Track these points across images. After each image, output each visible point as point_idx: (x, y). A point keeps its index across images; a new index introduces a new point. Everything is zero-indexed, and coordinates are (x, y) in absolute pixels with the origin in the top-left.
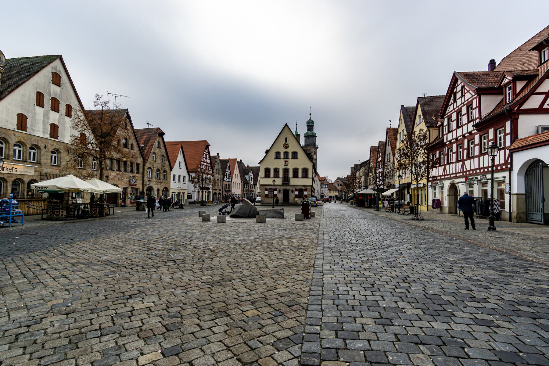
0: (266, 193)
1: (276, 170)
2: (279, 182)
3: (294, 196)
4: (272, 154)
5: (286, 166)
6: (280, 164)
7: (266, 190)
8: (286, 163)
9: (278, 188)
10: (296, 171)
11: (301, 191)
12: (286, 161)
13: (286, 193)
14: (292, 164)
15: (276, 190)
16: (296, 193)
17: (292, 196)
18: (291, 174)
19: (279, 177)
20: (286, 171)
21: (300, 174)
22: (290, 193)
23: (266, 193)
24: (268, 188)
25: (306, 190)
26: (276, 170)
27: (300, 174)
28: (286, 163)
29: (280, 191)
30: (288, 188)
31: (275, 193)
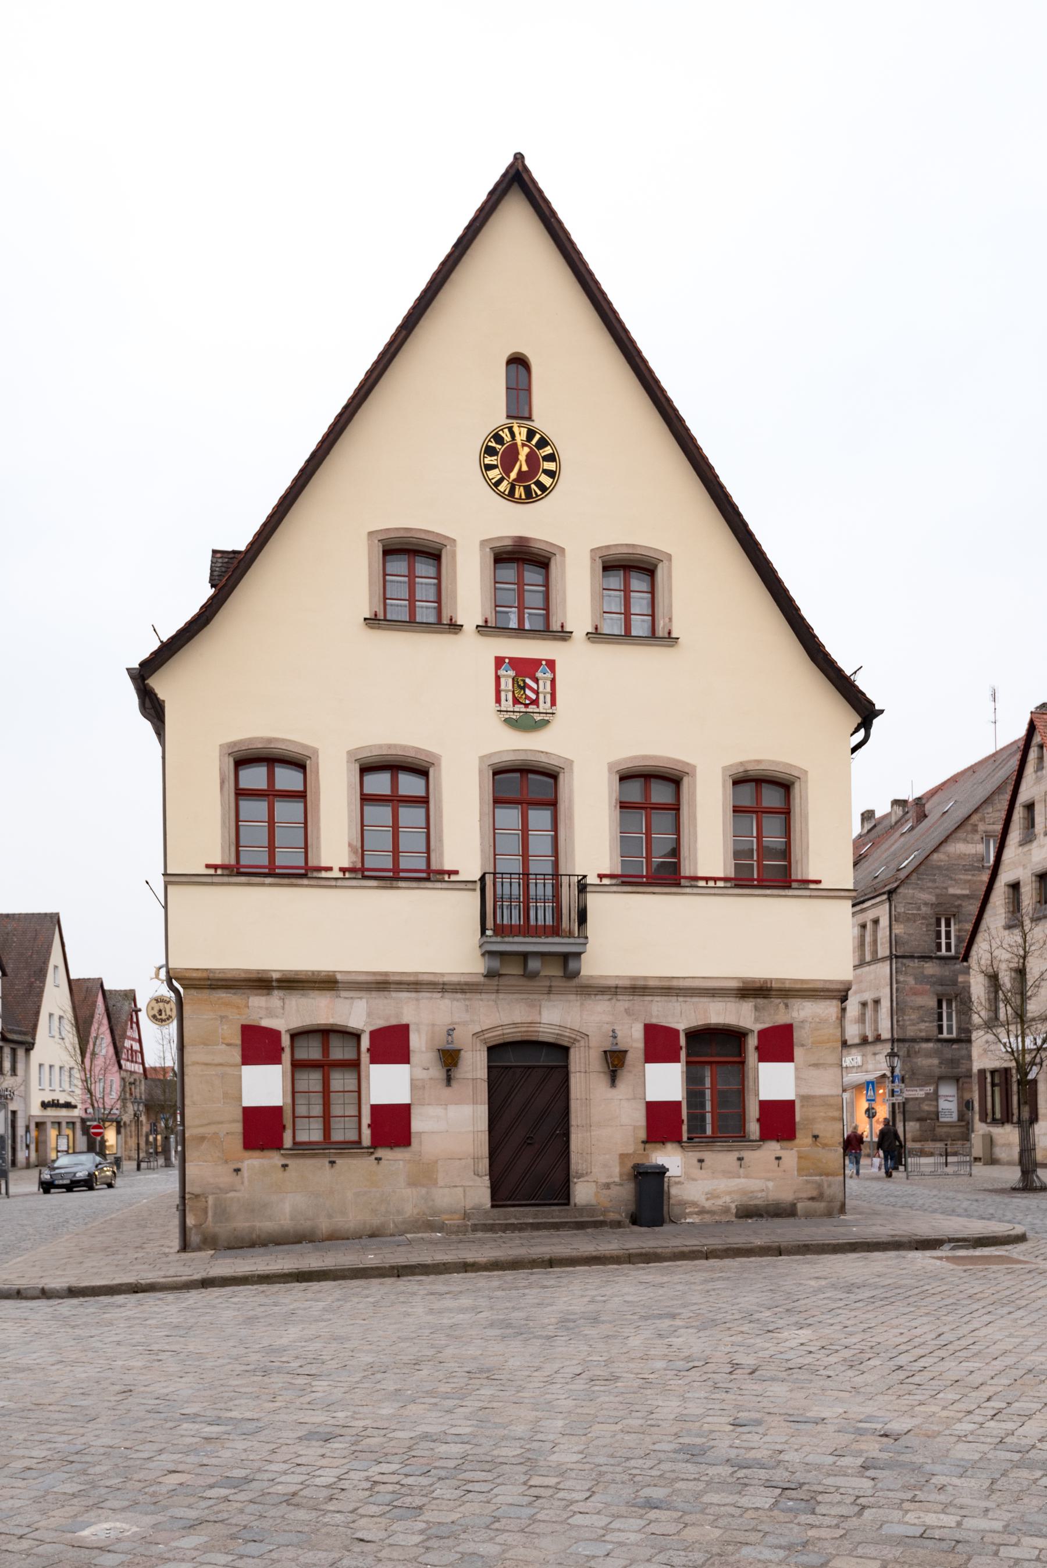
0: (265, 1085)
1: (396, 779)
2: (433, 934)
3: (633, 1119)
4: (331, 569)
5: (525, 724)
6: (442, 700)
7: (258, 1045)
8: (525, 687)
9: (425, 1020)
10: (652, 792)
11: (715, 1051)
12: (525, 668)
13: (528, 1088)
14: (606, 712)
15: (392, 1044)
16: (666, 1082)
17: (605, 1127)
18: (592, 836)
19: (432, 875)
20: (526, 787)
21: (710, 838)
22: (586, 1083)
23: (265, 1085)
24: (283, 1015)
25: (778, 1044)
26: (396, 779)
27: (710, 838)
28: (525, 687)
29: (450, 1059)
30: (553, 1016)
31: (387, 1084)
